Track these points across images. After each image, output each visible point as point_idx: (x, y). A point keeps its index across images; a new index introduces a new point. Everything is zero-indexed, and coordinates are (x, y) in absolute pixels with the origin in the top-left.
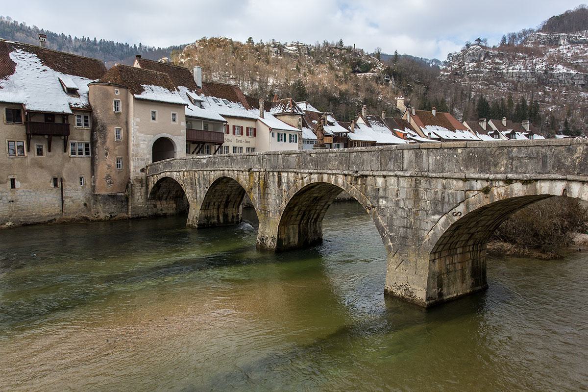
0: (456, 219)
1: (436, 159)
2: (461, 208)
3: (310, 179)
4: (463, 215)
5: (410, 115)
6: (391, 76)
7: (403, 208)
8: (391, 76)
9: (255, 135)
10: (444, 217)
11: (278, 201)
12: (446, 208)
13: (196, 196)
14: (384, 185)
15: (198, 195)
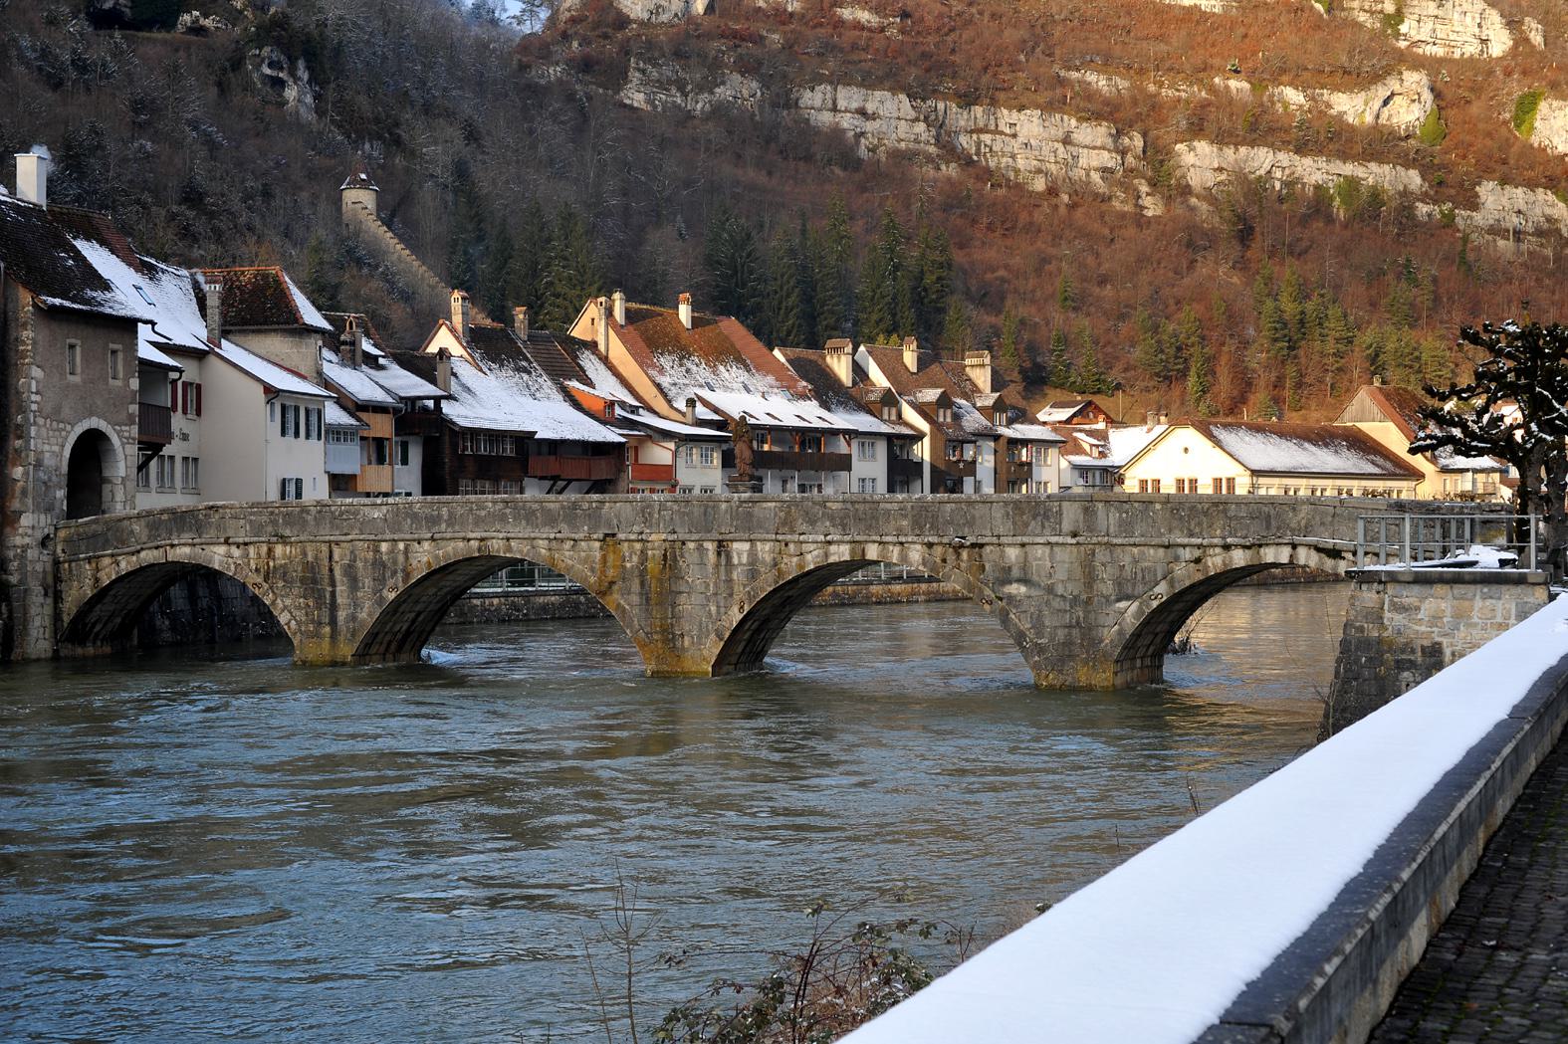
0: (1155, 604)
1: (1120, 516)
2: (1162, 589)
3: (827, 555)
4: (1165, 598)
5: (607, 324)
6: (292, 61)
7: (1062, 596)
8: (292, 61)
9: (199, 413)
10: (1136, 604)
11: (713, 609)
12: (1140, 589)
13: (333, 622)
14: (1022, 560)
15: (342, 615)
